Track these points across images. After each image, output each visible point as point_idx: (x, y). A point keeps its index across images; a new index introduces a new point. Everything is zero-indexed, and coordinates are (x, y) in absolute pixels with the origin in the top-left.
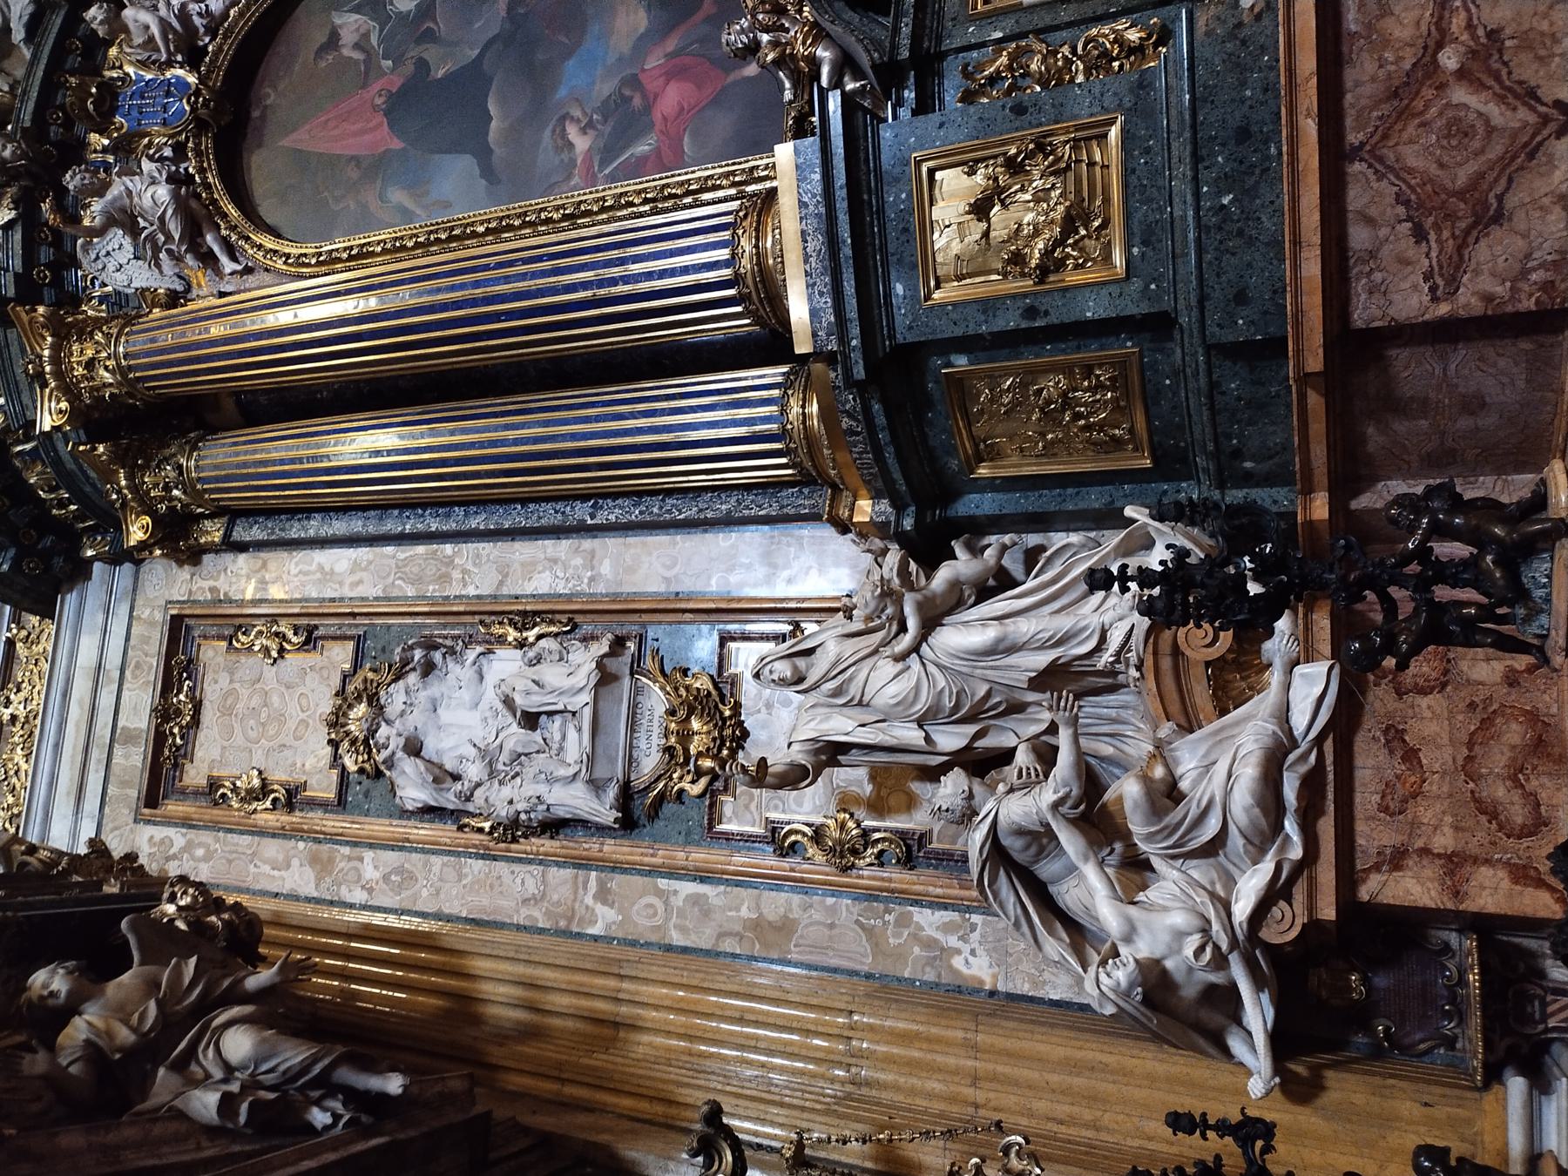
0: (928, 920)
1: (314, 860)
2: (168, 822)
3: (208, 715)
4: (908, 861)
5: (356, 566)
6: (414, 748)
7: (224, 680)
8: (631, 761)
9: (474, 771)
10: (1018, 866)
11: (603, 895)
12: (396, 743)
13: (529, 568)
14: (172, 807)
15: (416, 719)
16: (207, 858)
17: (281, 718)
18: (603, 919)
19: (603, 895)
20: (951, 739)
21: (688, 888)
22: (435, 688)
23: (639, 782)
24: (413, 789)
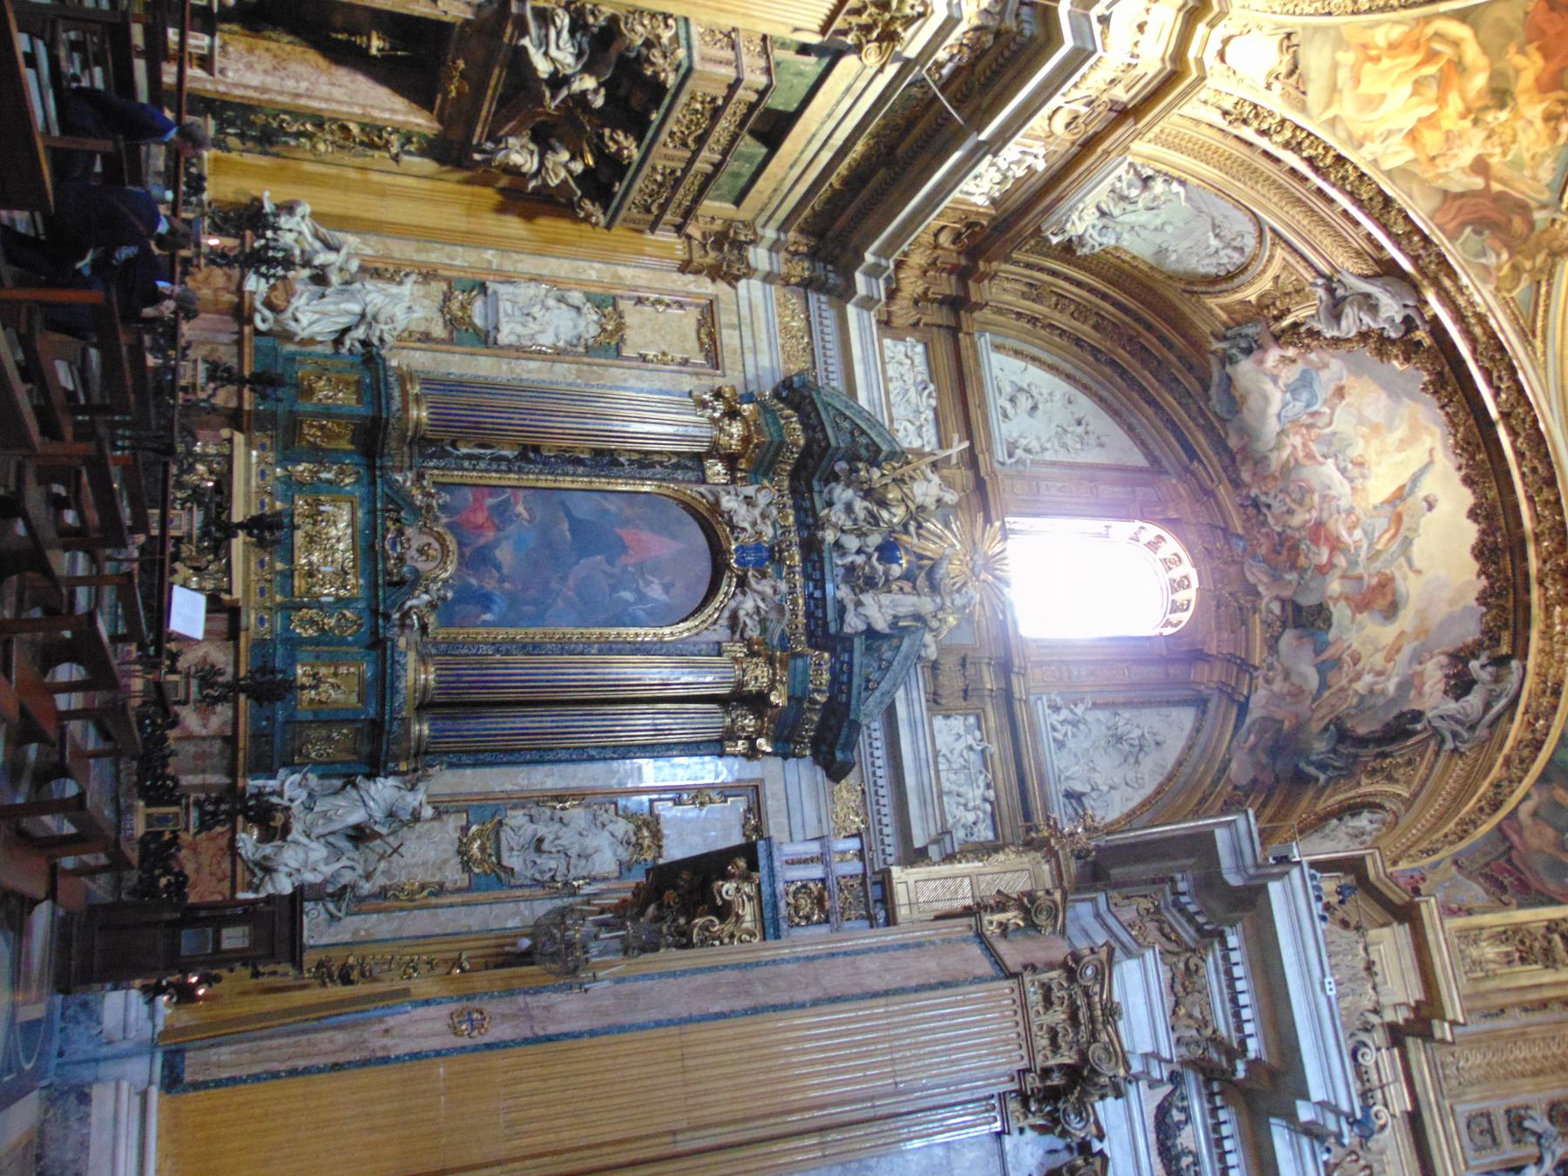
0: (368, 251)
1: (620, 278)
2: (698, 295)
3: (693, 335)
4: (376, 269)
5: (626, 380)
6: (578, 309)
7: (688, 347)
8: (485, 304)
9: (551, 302)
10: (330, 247)
11: (490, 262)
12: (585, 310)
13: (539, 370)
14: (704, 302)
15: (582, 323)
16: (674, 281)
17: (653, 330)
18: (489, 254)
19: (490, 262)
20: (357, 286)
21: (456, 263)
22: (575, 333)
23: (481, 297)
24: (576, 297)
